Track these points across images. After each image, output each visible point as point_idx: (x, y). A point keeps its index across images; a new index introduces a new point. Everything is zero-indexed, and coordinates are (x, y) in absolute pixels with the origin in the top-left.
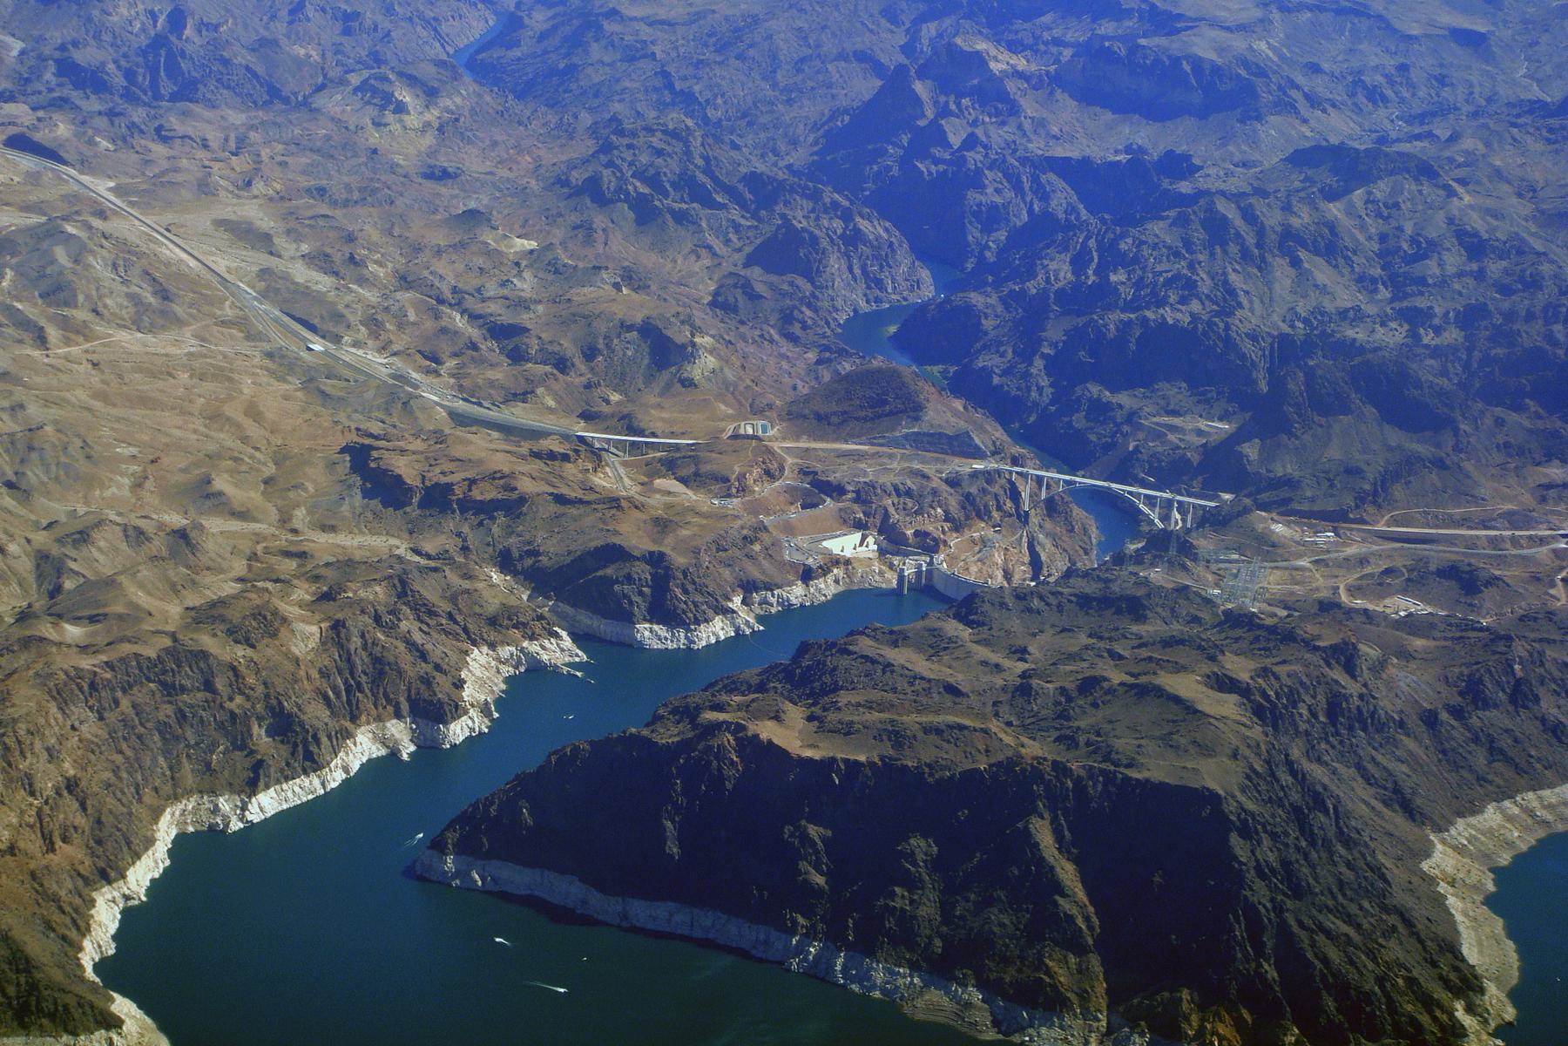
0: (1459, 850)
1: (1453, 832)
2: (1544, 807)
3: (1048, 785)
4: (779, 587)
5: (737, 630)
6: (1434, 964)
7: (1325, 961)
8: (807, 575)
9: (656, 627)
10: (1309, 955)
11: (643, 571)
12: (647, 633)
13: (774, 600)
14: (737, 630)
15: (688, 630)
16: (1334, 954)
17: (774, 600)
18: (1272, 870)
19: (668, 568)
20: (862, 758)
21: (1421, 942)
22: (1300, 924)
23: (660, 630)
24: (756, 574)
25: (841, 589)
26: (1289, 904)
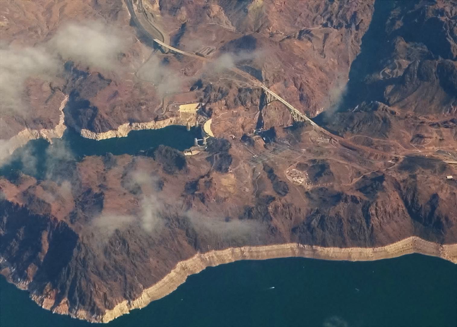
0: (202, 260)
1: (206, 254)
2: (249, 252)
3: (51, 223)
4: (143, 122)
5: (117, 135)
6: (125, 290)
7: (80, 284)
8: (156, 119)
9: (87, 131)
10: (78, 282)
11: (89, 111)
12: (84, 132)
13: (140, 126)
14: (117, 135)
15: (97, 134)
16: (83, 283)
17: (140, 126)
18: (80, 259)
19: (96, 113)
20: (21, 204)
21: (126, 283)
22: (80, 274)
23: (89, 132)
24: (136, 116)
25: (171, 124)
26: (80, 268)
